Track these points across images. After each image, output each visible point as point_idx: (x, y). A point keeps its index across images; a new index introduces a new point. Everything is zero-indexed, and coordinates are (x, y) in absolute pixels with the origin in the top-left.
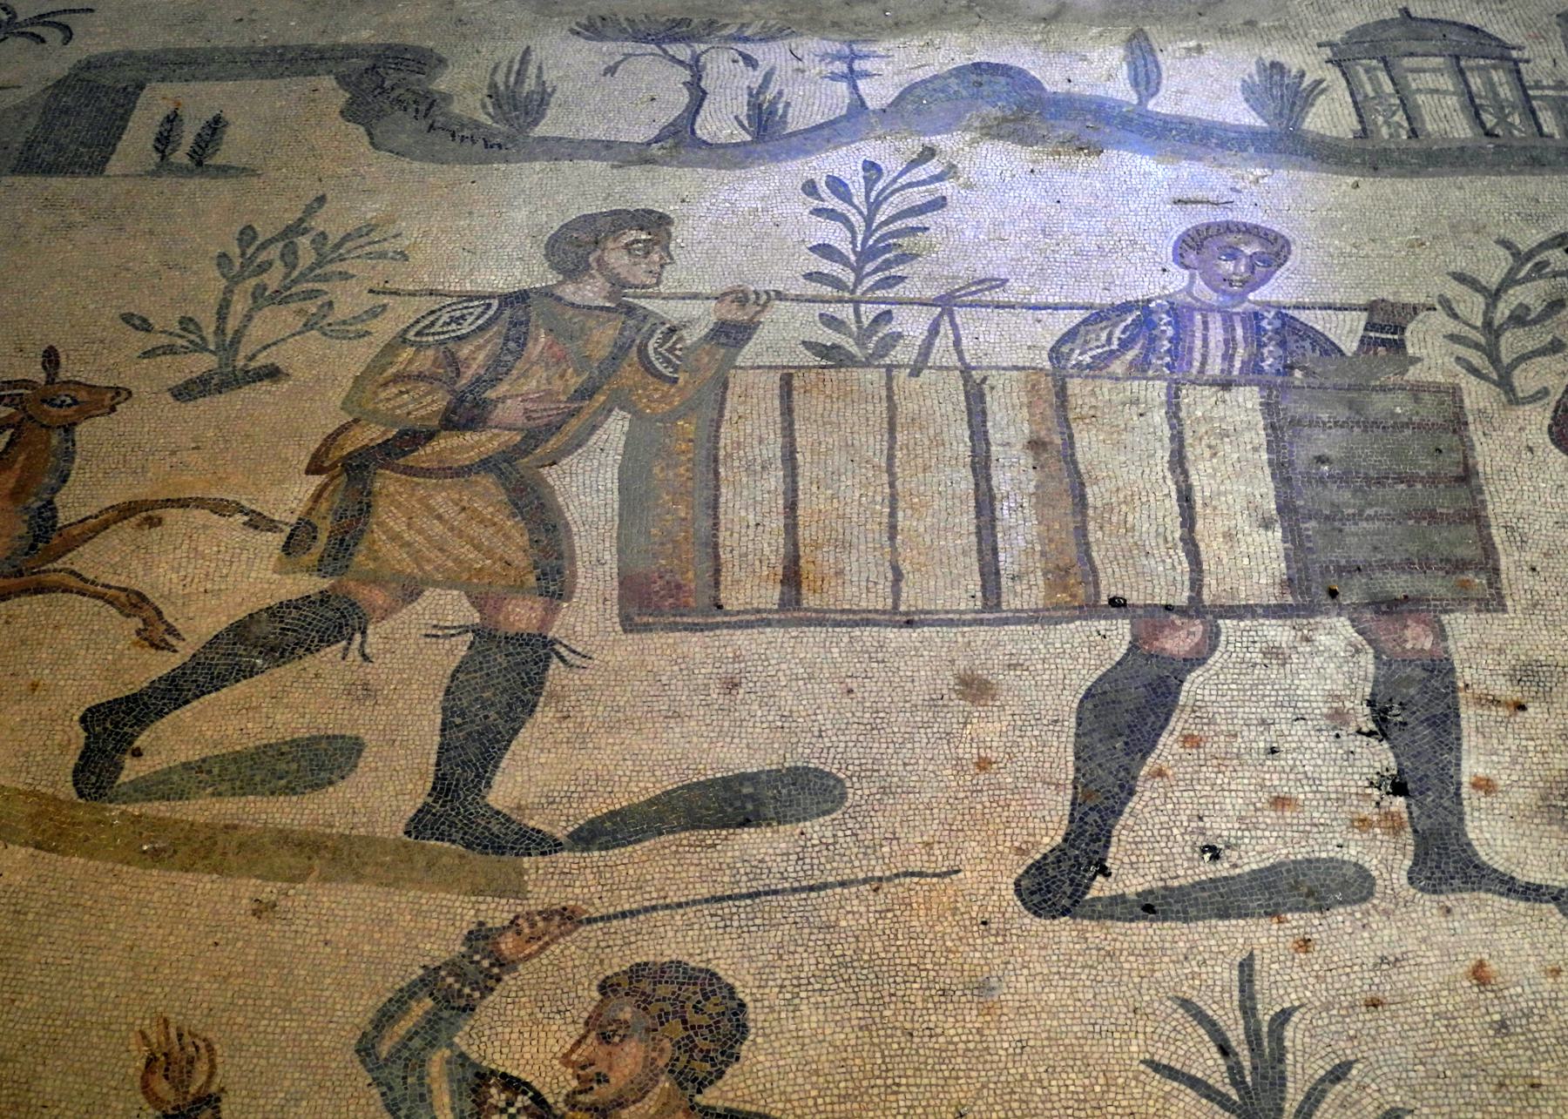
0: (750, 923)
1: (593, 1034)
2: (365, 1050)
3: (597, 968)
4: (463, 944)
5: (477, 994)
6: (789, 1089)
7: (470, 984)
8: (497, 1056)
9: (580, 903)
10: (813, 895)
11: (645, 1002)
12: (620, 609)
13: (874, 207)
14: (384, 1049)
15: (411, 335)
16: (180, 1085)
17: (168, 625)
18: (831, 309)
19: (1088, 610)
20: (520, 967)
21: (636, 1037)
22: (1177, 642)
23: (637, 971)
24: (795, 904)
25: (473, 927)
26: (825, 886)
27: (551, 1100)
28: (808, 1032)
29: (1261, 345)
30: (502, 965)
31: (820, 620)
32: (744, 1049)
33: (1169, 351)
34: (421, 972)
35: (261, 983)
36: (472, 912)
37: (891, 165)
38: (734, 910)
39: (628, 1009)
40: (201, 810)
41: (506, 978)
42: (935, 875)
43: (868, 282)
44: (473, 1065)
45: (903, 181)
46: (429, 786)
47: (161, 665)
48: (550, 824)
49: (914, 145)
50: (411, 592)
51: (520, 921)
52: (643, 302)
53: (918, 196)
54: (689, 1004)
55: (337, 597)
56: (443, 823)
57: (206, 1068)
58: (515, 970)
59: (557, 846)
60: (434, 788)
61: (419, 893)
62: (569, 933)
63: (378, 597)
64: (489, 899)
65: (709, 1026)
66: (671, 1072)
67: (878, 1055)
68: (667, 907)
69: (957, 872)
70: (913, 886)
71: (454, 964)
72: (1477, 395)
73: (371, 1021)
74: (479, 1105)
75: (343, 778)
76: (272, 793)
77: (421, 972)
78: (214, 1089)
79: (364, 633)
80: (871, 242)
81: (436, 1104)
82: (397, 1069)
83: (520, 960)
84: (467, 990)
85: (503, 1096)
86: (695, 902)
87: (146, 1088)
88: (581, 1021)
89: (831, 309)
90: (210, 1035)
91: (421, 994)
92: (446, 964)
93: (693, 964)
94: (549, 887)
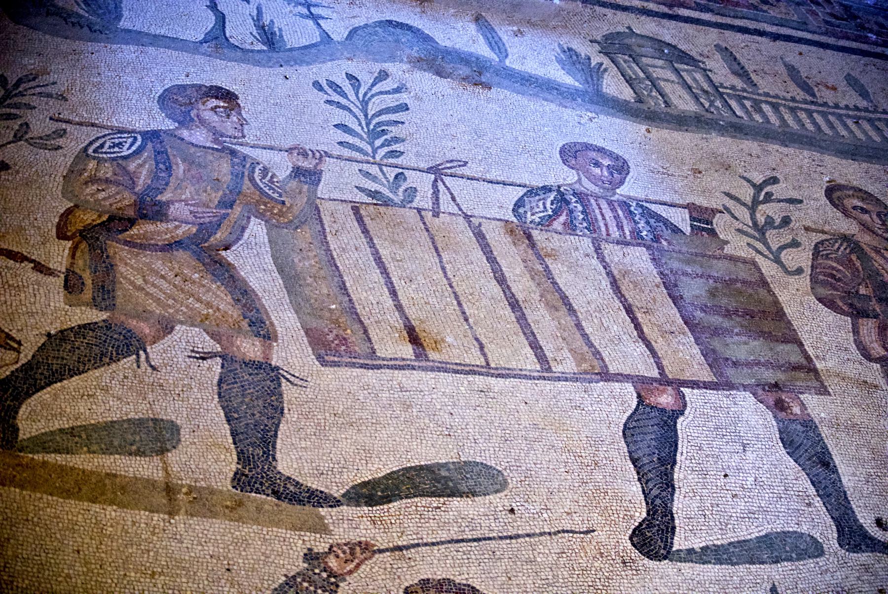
0: (483, 557)
3: (398, 581)
4: (304, 562)
7: (320, 588)
9: (368, 539)
10: (514, 541)
12: (313, 350)
13: (365, 103)
15: (90, 151)
17: (6, 333)
18: (365, 167)
19: (606, 376)
20: (348, 578)
22: (666, 400)
24: (504, 546)
25: (305, 551)
26: (517, 536)
29: (636, 223)
30: (335, 577)
31: (443, 368)
33: (584, 219)
34: (284, 578)
35: (178, 580)
36: (301, 542)
37: (366, 80)
38: (469, 548)
41: (341, 584)
42: (581, 533)
43: (382, 152)
45: (375, 89)
46: (235, 457)
48: (327, 487)
49: (377, 67)
50: (166, 328)
52: (238, 148)
53: (390, 101)
55: (116, 325)
56: (255, 483)
58: (345, 580)
59: (337, 503)
60: (239, 459)
61: (260, 527)
62: (370, 558)
63: (145, 329)
64: (308, 534)
68: (426, 544)
69: (594, 531)
70: (570, 539)
71: (304, 575)
72: (768, 268)
75: (174, 447)
77: (284, 578)
79: (145, 351)
80: (371, 127)
83: (346, 574)
86: (442, 543)
89: (365, 167)
92: (298, 574)
93: (457, 581)
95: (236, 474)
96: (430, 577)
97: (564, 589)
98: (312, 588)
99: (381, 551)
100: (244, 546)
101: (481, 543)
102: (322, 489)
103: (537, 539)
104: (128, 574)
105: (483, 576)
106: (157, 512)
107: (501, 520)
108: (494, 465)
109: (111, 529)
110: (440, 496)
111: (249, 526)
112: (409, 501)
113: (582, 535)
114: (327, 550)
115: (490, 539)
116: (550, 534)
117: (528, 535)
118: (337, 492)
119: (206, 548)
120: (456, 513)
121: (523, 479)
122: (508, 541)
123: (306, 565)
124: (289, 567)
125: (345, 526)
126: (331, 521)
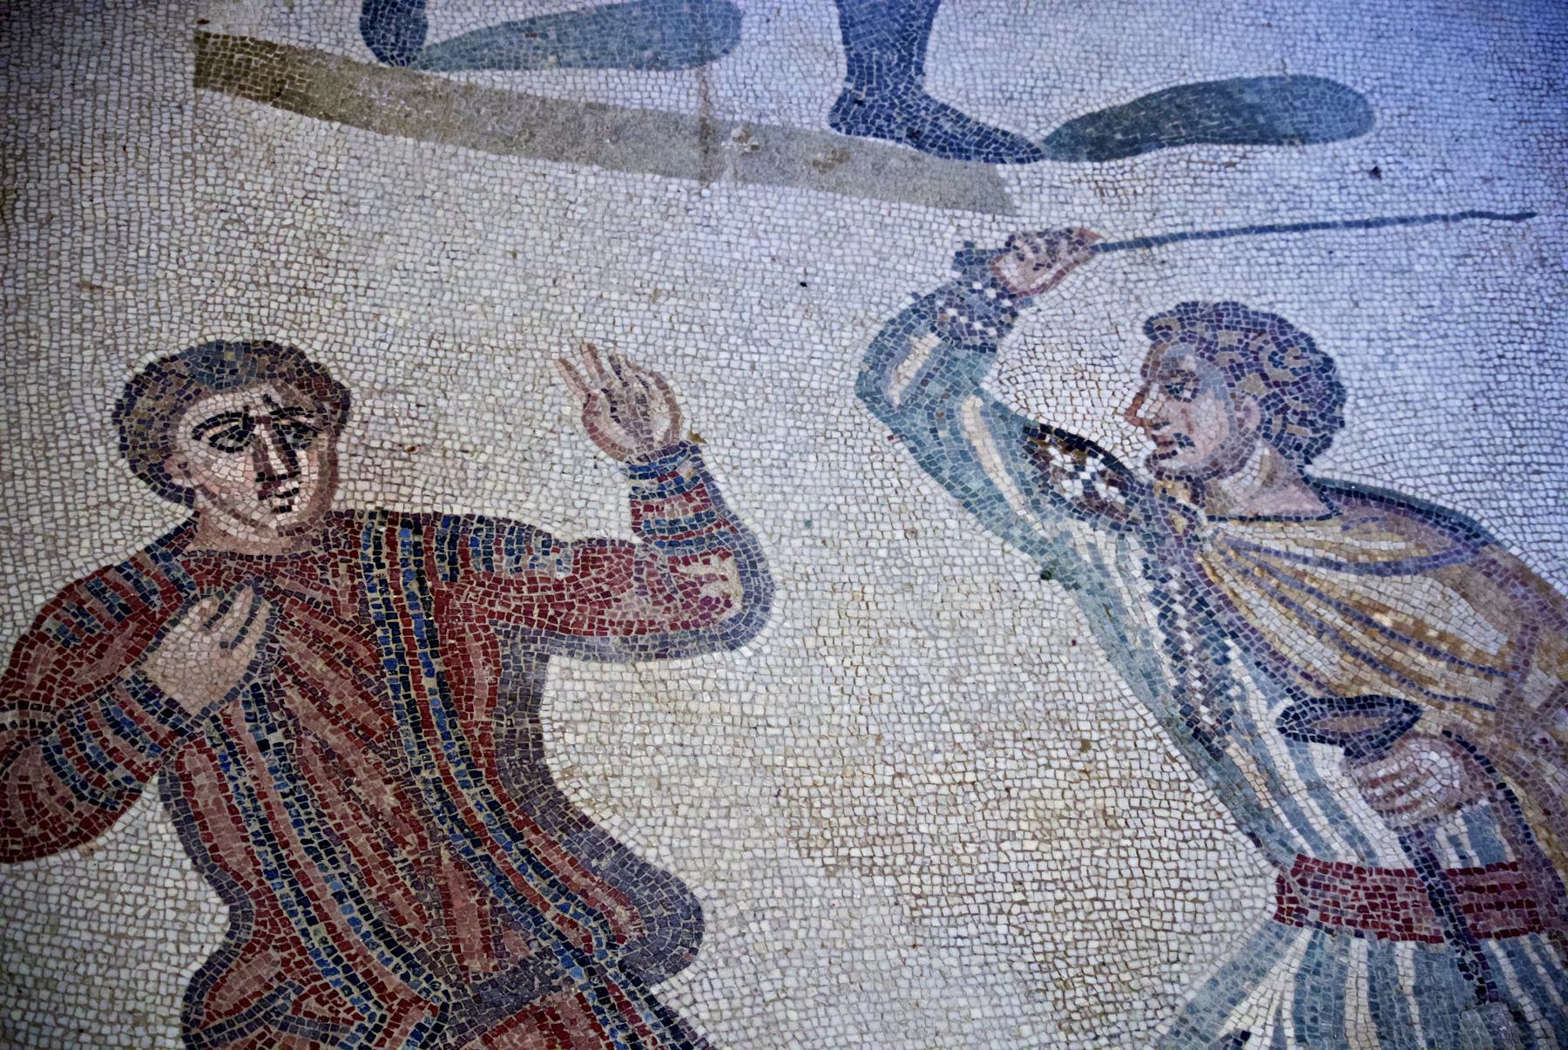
0: (1307, 261)
1: (1155, 387)
3: (1135, 305)
4: (954, 268)
5: (992, 331)
6: (1414, 463)
7: (980, 318)
8: (1043, 408)
9: (1087, 225)
10: (1372, 231)
11: (1208, 351)
14: (895, 393)
16: (638, 425)
20: (1036, 299)
21: (1210, 392)
23: (1187, 311)
24: (1353, 241)
25: (960, 247)
26: (1381, 222)
27: (1129, 465)
28: (1417, 397)
30: (1011, 297)
32: (1346, 411)
34: (911, 300)
35: (703, 305)
36: (953, 229)
38: (1283, 244)
39: (1190, 357)
41: (1022, 312)
42: (1506, 218)
44: (1015, 417)
48: (1017, 124)
51: (1018, 243)
54: (1264, 356)
56: (877, 116)
57: (665, 409)
58: (1031, 304)
59: (1034, 154)
61: (876, 202)
62: (1086, 261)
64: (969, 214)
65: (1295, 384)
66: (1266, 436)
67: (1505, 427)
68: (1198, 235)
69: (1532, 215)
70: (1485, 229)
71: (951, 293)
73: (866, 360)
74: (1041, 468)
76: (639, 67)
77: (911, 300)
78: (684, 436)
81: (987, 464)
82: (920, 418)
83: (1033, 291)
84: (978, 326)
85: (1068, 458)
86: (1232, 233)
87: (592, 430)
88: (1137, 370)
90: (657, 368)
91: (920, 328)
92: (940, 291)
93: (1252, 308)
94: (1041, 203)
95: (841, 99)
96: (1200, 298)
97: (1462, 327)
98: (964, 320)
99: (1107, 248)
100: (840, 237)
101: (1307, 234)
102: (1007, 128)
103: (1418, 229)
104: (606, 295)
105: (1304, 298)
106: (678, 175)
107: (1353, 190)
108: (1349, 84)
109: (584, 210)
110: (1236, 142)
111: (855, 199)
112: (1176, 150)
113: (1509, 223)
114: (1002, 245)
115: (1326, 226)
116: (1445, 218)
117: (1403, 221)
118: (1035, 133)
119: (765, 243)
120: (1264, 176)
121: (1404, 110)
122: (1361, 231)
123: (957, 275)
124: (924, 278)
125: (1044, 198)
126: (1017, 189)
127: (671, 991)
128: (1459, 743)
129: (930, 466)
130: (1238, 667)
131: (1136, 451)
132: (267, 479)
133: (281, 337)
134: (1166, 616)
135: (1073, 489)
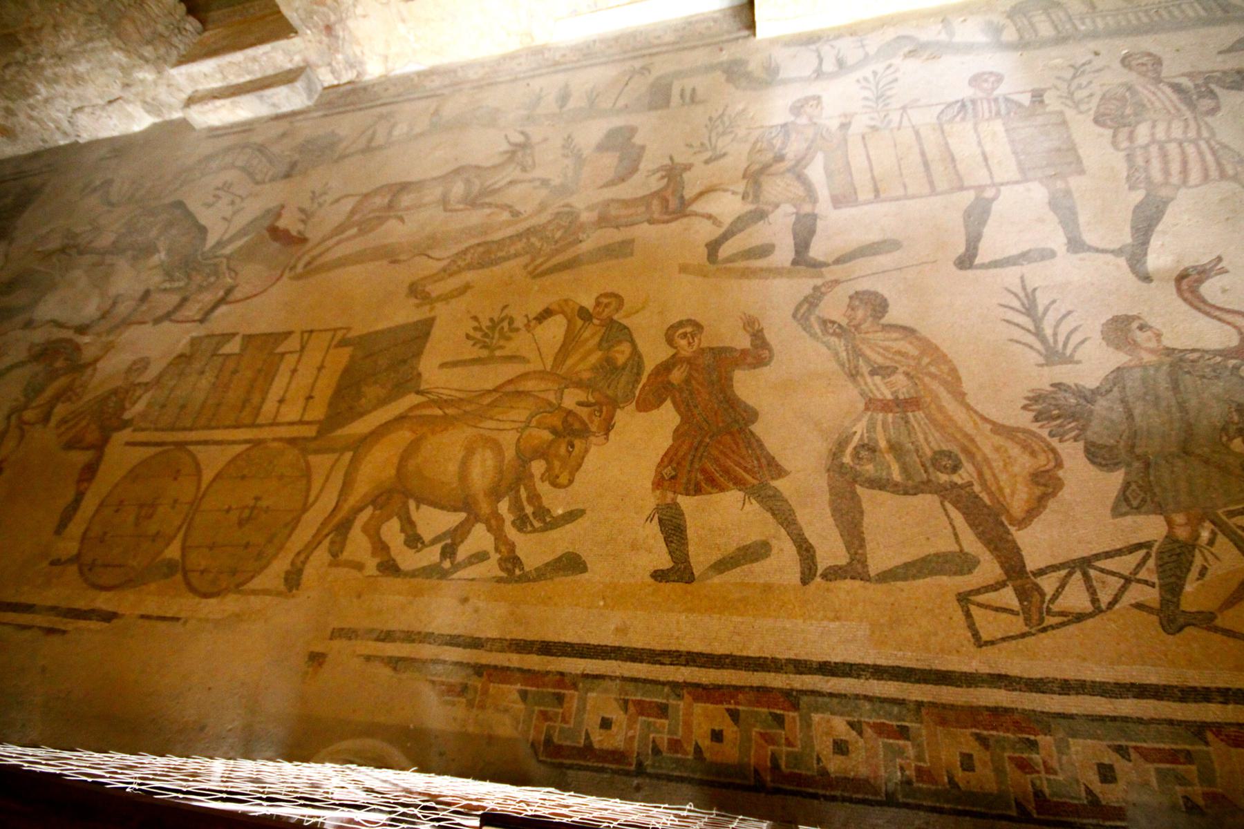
2: (794, 316)
11: (861, 300)
40: (741, 264)
47: (722, 230)
127: (753, 428)
128: (907, 374)
129: (805, 329)
130: (861, 362)
131: (844, 322)
132: (689, 343)
133: (693, 318)
134: (848, 354)
135: (831, 331)
